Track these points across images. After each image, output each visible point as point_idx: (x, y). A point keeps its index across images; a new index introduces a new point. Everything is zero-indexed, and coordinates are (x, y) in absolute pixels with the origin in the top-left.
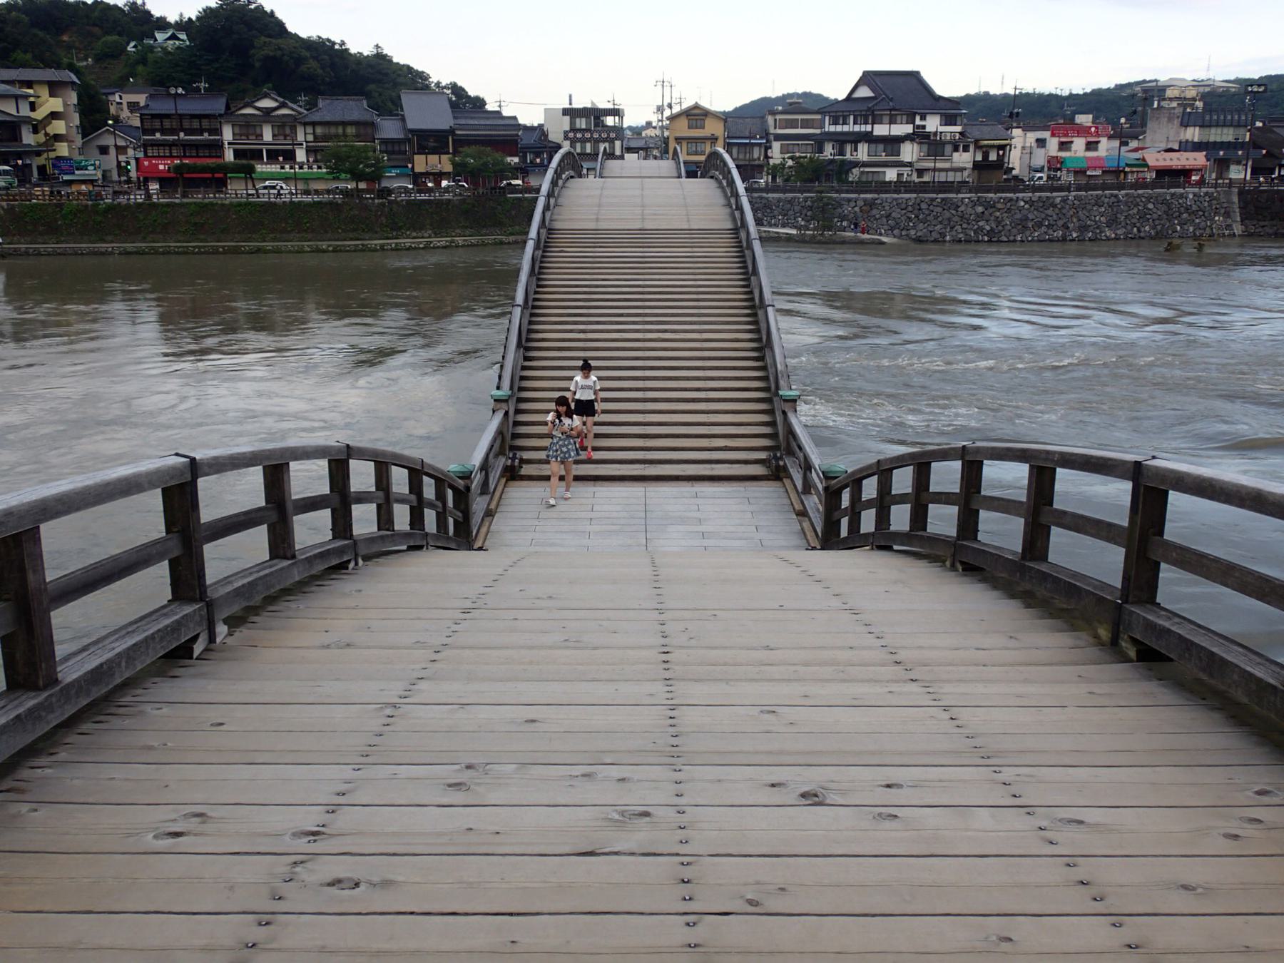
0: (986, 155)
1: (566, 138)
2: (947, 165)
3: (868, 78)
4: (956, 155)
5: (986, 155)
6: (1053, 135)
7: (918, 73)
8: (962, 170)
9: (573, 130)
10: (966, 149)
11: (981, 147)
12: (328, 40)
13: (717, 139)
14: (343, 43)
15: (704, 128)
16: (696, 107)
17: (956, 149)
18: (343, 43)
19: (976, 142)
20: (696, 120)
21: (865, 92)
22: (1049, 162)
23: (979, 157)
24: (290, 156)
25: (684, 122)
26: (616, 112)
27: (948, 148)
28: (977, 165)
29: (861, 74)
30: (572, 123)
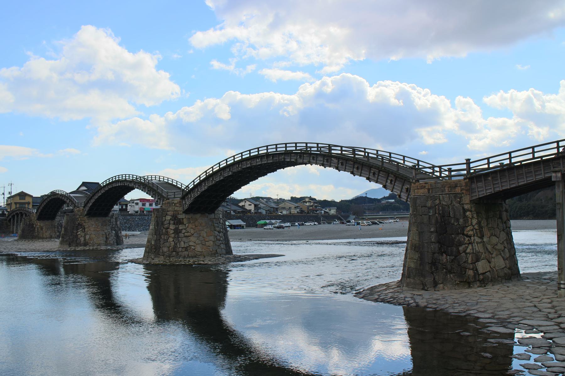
0: (122, 207)
3: (84, 184)
5: (122, 207)
6: (140, 201)
8: (116, 211)
13: (30, 203)
15: (25, 199)
20: (22, 197)
22: (140, 209)
25: (18, 198)
28: (120, 209)
29: (82, 183)
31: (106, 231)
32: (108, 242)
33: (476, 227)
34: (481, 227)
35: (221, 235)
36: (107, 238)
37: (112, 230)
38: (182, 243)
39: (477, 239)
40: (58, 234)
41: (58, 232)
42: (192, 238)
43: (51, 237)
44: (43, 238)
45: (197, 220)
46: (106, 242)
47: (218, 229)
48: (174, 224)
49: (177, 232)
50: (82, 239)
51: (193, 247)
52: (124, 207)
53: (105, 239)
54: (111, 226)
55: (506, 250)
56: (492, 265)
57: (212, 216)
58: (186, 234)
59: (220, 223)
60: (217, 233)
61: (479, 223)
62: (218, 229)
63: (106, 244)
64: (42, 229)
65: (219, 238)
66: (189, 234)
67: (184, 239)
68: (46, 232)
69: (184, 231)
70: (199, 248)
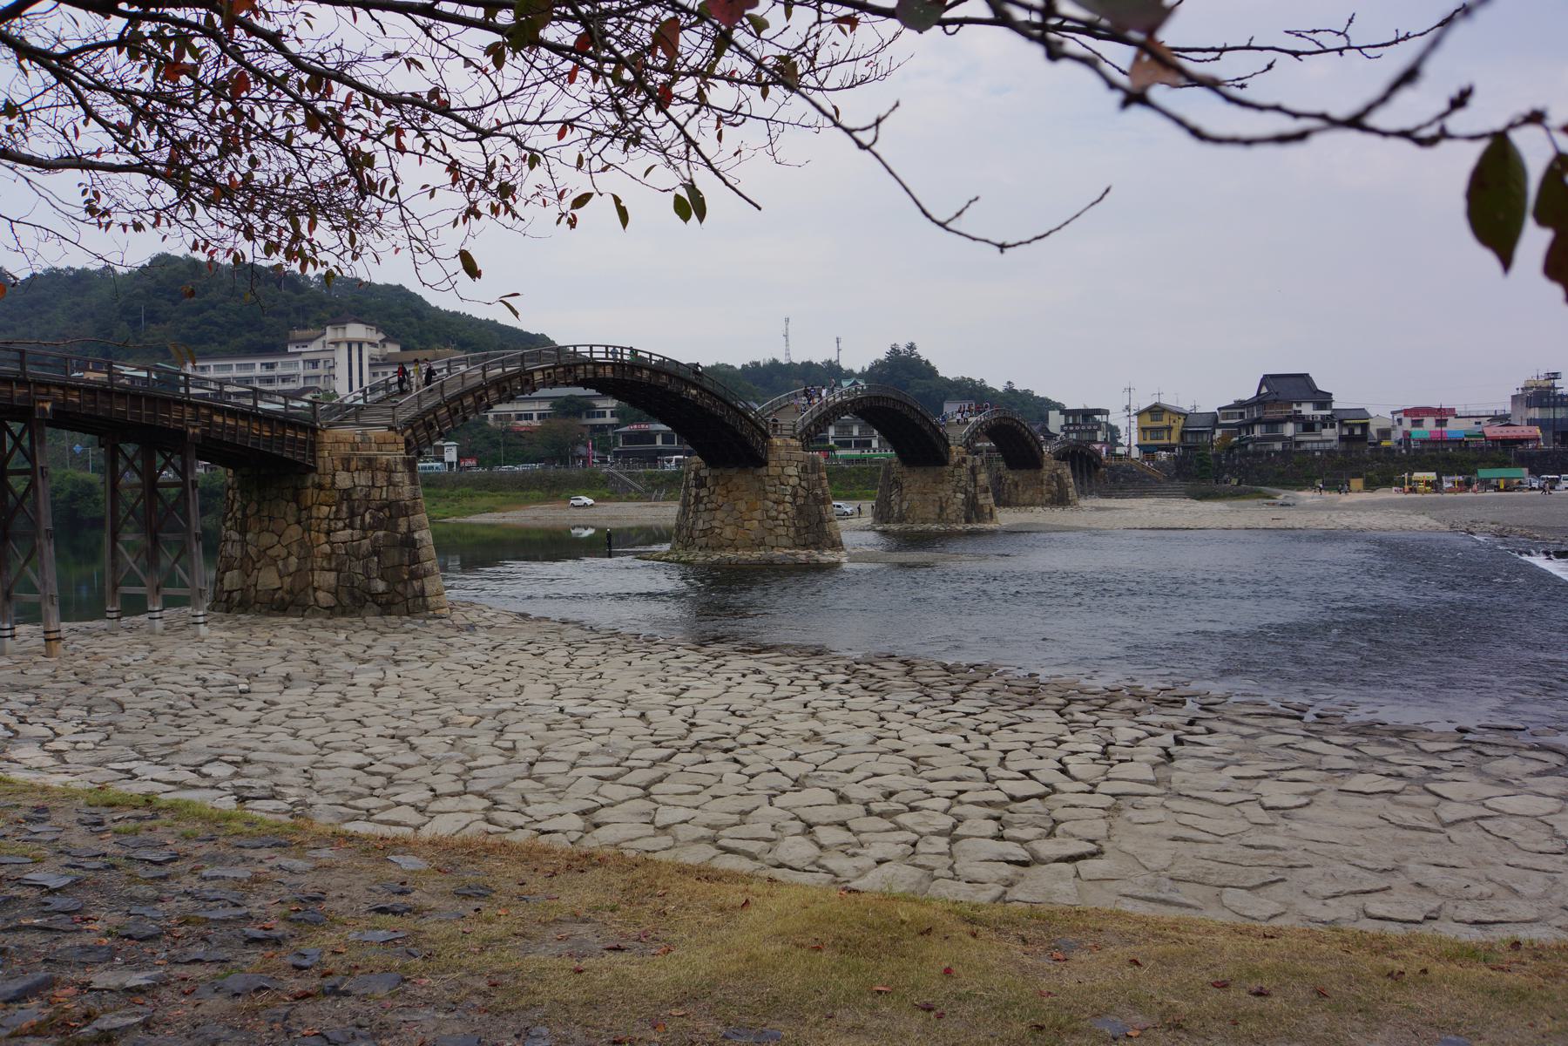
0: (1351, 431)
1: (1062, 430)
2: (1318, 438)
3: (1267, 380)
4: (1324, 431)
5: (1351, 431)
7: (1305, 377)
9: (1067, 424)
10: (1333, 426)
11: (1347, 425)
12: (969, 379)
14: (982, 381)
16: (1156, 406)
17: (1325, 426)
18: (982, 381)
19: (1341, 422)
21: (1264, 390)
23: (1345, 432)
24: (868, 444)
25: (1147, 417)
26: (1107, 412)
27: (1318, 427)
28: (1342, 438)
30: (1066, 420)
31: (942, 494)
32: (944, 516)
33: (239, 515)
34: (244, 515)
35: (781, 508)
36: (942, 509)
37: (955, 492)
38: (701, 522)
39: (235, 536)
40: (1048, 496)
41: (1050, 492)
42: (719, 515)
43: (1033, 504)
44: (1017, 505)
45: (730, 480)
46: (940, 516)
47: (773, 497)
48: (696, 487)
49: (698, 499)
50: (896, 509)
51: (717, 530)
52: (1358, 432)
53: (938, 510)
54: (954, 483)
55: (293, 560)
56: (251, 581)
57: (763, 471)
58: (709, 506)
59: (782, 484)
60: (770, 504)
61: (244, 509)
62: (773, 497)
63: (940, 518)
64: (1016, 485)
65: (774, 513)
66: (714, 505)
67: (705, 516)
68: (1024, 492)
69: (705, 500)
70: (728, 532)
